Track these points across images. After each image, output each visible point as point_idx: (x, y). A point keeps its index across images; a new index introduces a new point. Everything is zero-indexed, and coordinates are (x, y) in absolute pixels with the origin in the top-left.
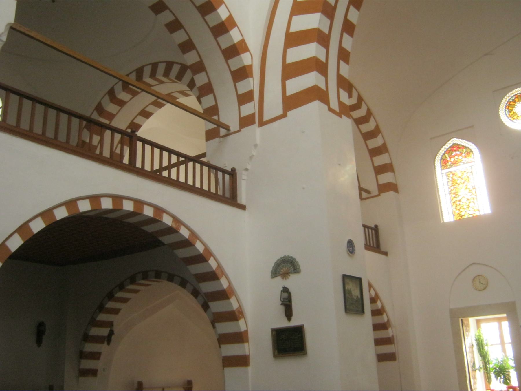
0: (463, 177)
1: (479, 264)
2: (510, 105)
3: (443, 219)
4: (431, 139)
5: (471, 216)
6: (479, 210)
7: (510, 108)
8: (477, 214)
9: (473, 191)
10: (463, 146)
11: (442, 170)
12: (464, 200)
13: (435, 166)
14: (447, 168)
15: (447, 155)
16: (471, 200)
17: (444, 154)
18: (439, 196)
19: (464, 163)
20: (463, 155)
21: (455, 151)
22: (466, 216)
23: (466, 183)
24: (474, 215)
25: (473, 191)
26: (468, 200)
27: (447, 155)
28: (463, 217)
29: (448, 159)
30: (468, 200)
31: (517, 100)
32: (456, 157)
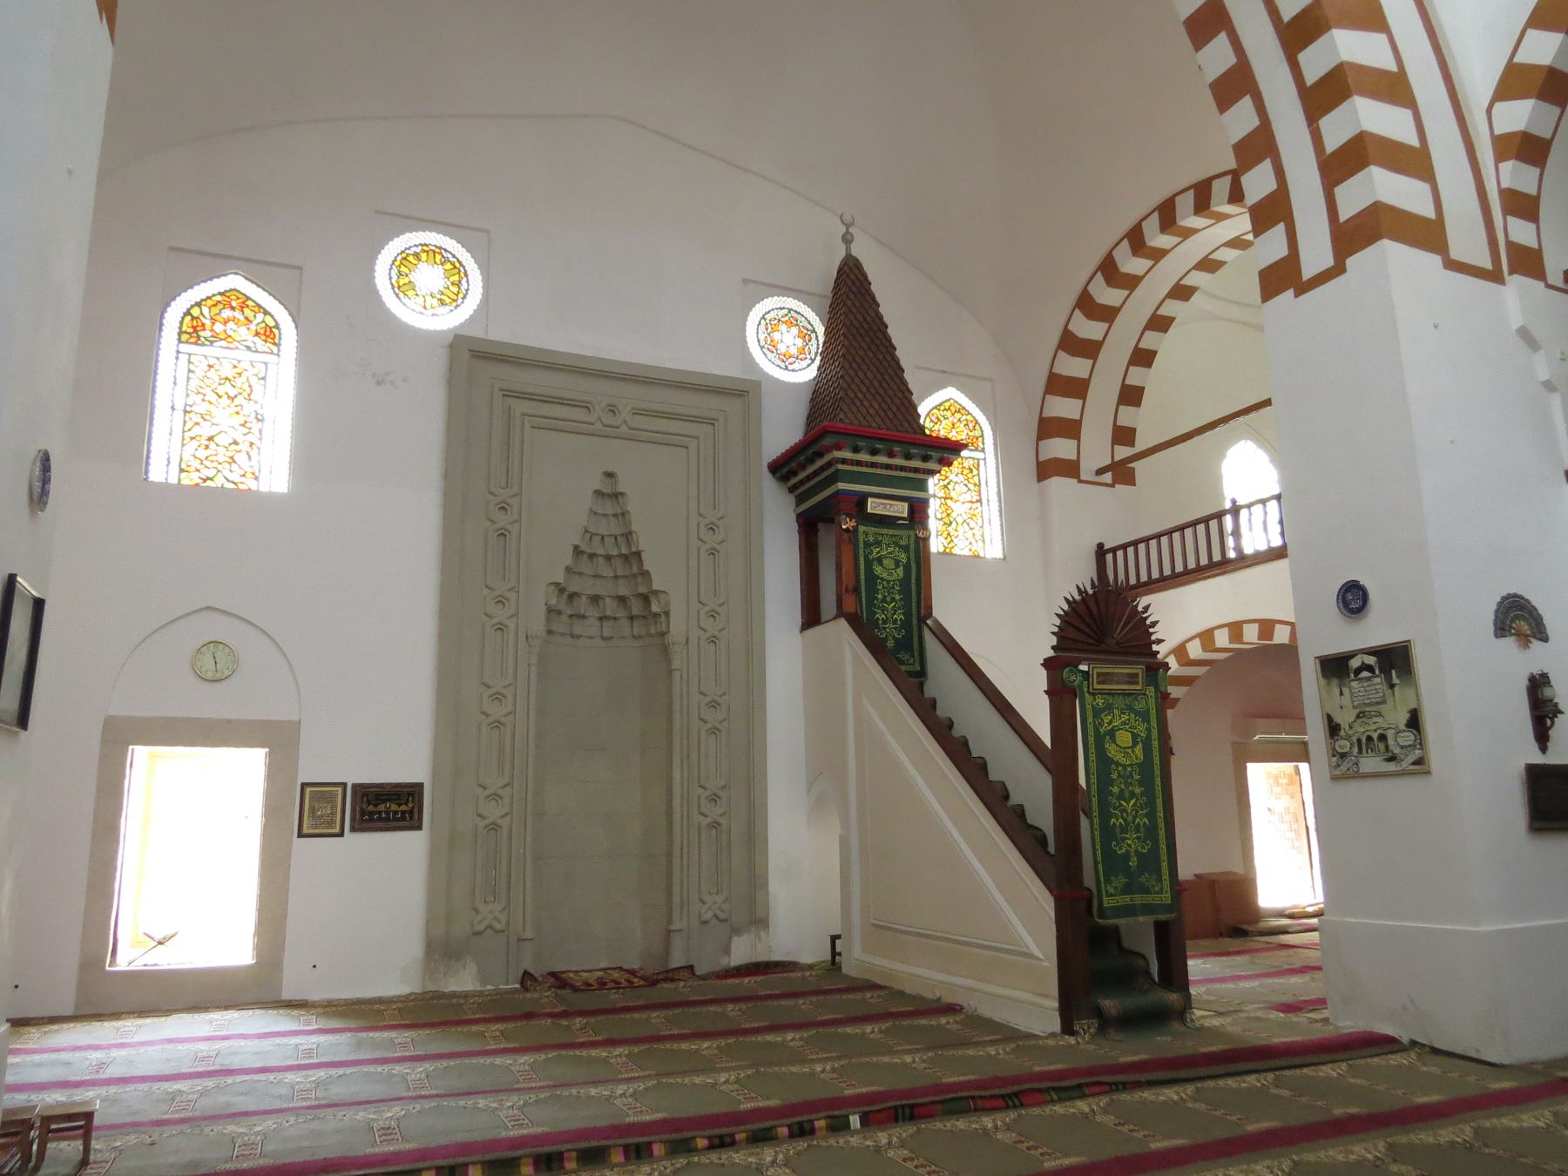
0: (239, 382)
1: (236, 616)
2: (405, 260)
3: (147, 472)
4: (171, 249)
5: (232, 486)
6: (256, 478)
7: (403, 269)
8: (253, 485)
9: (256, 426)
10: (259, 306)
11: (180, 341)
12: (223, 440)
13: (161, 324)
14: (195, 343)
15: (205, 310)
16: (244, 446)
17: (198, 304)
18: (153, 407)
19: (248, 348)
20: (253, 327)
21: (233, 308)
22: (219, 482)
23: (238, 400)
24: (241, 487)
25: (256, 426)
26: (235, 443)
27: (205, 310)
28: (209, 483)
29: (208, 323)
30: (235, 443)
31: (424, 256)
32: (231, 324)
